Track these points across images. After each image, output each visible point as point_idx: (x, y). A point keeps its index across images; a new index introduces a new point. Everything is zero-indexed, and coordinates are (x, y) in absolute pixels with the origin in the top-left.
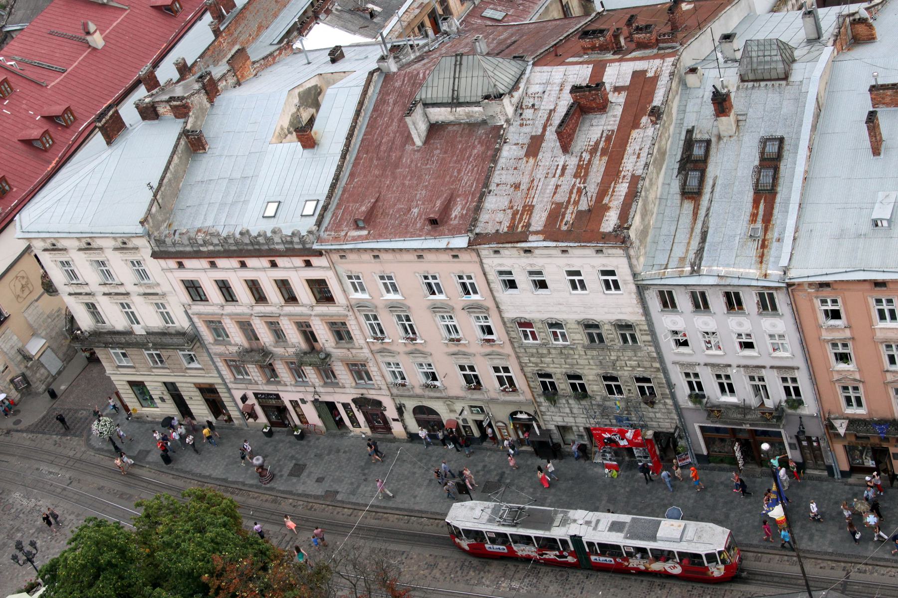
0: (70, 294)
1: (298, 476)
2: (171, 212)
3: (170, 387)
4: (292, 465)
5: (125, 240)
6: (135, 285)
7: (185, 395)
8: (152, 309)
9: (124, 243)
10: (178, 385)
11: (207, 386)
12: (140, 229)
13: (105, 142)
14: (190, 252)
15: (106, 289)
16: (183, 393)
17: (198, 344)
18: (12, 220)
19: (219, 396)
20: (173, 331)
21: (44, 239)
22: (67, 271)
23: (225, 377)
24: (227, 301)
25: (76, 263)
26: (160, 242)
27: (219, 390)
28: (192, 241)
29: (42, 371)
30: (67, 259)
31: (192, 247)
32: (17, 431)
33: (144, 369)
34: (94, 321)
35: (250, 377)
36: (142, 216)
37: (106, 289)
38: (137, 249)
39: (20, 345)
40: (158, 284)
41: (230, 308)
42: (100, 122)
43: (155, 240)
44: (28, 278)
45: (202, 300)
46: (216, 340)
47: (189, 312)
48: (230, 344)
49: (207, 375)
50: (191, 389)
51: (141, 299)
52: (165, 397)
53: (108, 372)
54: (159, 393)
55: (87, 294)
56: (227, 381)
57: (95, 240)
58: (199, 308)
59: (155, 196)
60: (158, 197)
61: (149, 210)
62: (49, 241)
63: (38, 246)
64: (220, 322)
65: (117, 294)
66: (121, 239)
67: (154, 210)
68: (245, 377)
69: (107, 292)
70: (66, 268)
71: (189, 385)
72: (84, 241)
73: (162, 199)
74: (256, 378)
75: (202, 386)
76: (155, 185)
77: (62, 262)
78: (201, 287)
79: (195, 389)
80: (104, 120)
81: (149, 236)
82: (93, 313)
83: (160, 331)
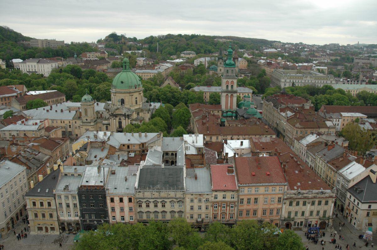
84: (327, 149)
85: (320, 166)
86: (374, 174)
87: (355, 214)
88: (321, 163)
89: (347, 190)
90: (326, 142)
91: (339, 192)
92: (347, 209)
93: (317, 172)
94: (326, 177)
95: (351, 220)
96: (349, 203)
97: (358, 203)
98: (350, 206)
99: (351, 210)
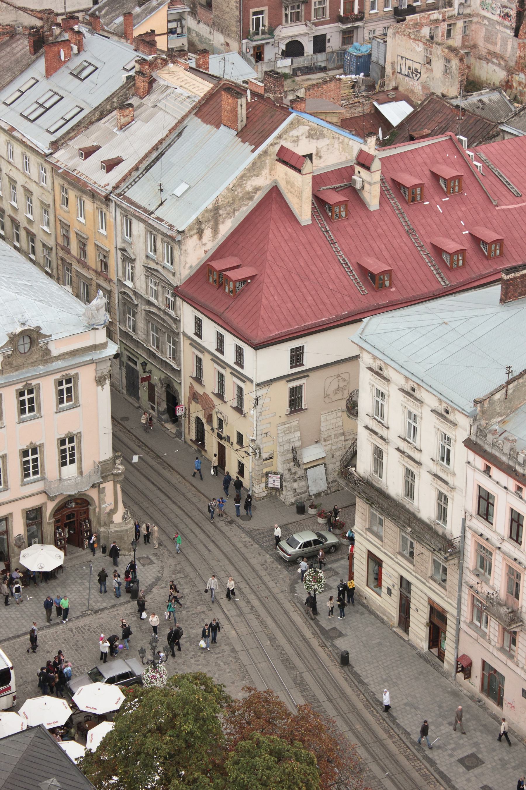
0: (367, 427)
1: (468, 768)
2: (514, 410)
3: (404, 585)
4: (470, 752)
5: (449, 409)
6: (432, 459)
7: (414, 603)
8: (434, 496)
9: (447, 412)
10: (413, 588)
11: (440, 610)
12: (469, 407)
13: (499, 298)
14: (504, 463)
15: (403, 446)
16: (412, 600)
17: (456, 561)
18: (360, 320)
19: (446, 628)
20: (440, 532)
21: (375, 358)
22: (377, 402)
23: (462, 612)
24: (511, 537)
25: (391, 399)
26: (481, 432)
27: (448, 622)
28: (513, 454)
29: (303, 483)
30: (384, 391)
31: (509, 458)
32: (240, 527)
33: (391, 550)
34: (373, 468)
35: (486, 631)
36: (480, 395)
37: (403, 446)
38: (455, 425)
39: (298, 444)
40: (454, 474)
41: (509, 547)
42: (507, 274)
43: (478, 428)
44: (348, 383)
45: (487, 519)
46: (476, 569)
47: (468, 523)
48: (487, 582)
49: (446, 598)
50: (423, 601)
51: (430, 477)
52: (393, 591)
53: (355, 527)
54: (391, 583)
55: (382, 438)
56: (462, 619)
57: (422, 390)
58: (479, 525)
59: (509, 383)
60: (511, 386)
61: (492, 394)
62: (378, 362)
63: (366, 360)
64: (491, 554)
65: (410, 457)
66: (446, 405)
67: (497, 396)
68: (483, 627)
69: (401, 448)
70: (378, 400)
71: (424, 596)
72: (411, 383)
73: (514, 391)
74: (492, 636)
75: (435, 605)
76: (516, 374)
77: (378, 391)
78: (493, 506)
79: (426, 604)
80: (512, 275)
81: (475, 420)
82: (376, 460)
83: (427, 521)
84: (41, 65)
85: (21, 180)
86: (299, 171)
87: (236, 415)
88: (18, 161)
89: (177, 292)
90: (39, 23)
91: (143, 307)
92: (195, 396)
93: (13, 220)
94: (60, 241)
95: (222, 449)
96: (199, 361)
97: (239, 352)
98: (204, 379)
99: (216, 401)
